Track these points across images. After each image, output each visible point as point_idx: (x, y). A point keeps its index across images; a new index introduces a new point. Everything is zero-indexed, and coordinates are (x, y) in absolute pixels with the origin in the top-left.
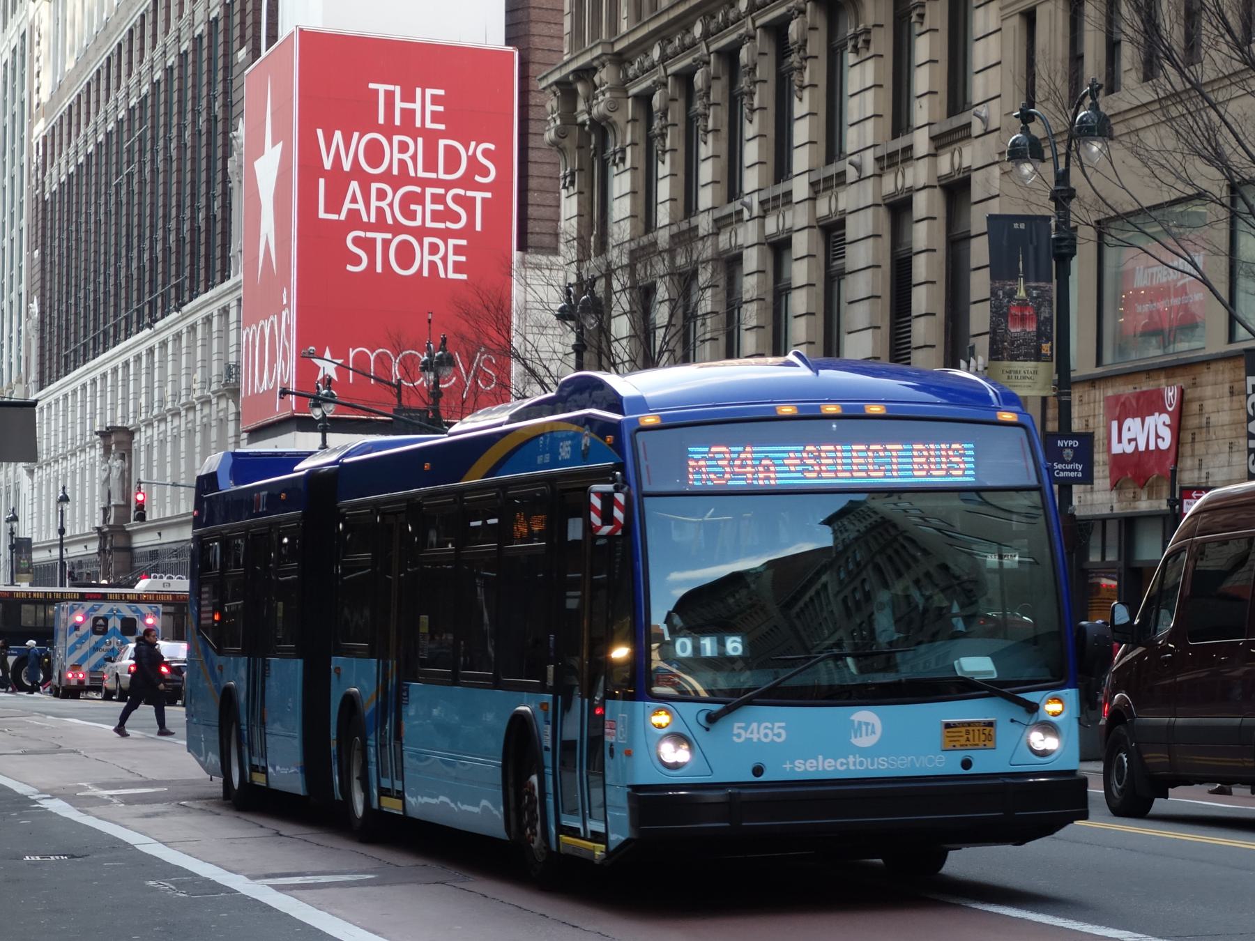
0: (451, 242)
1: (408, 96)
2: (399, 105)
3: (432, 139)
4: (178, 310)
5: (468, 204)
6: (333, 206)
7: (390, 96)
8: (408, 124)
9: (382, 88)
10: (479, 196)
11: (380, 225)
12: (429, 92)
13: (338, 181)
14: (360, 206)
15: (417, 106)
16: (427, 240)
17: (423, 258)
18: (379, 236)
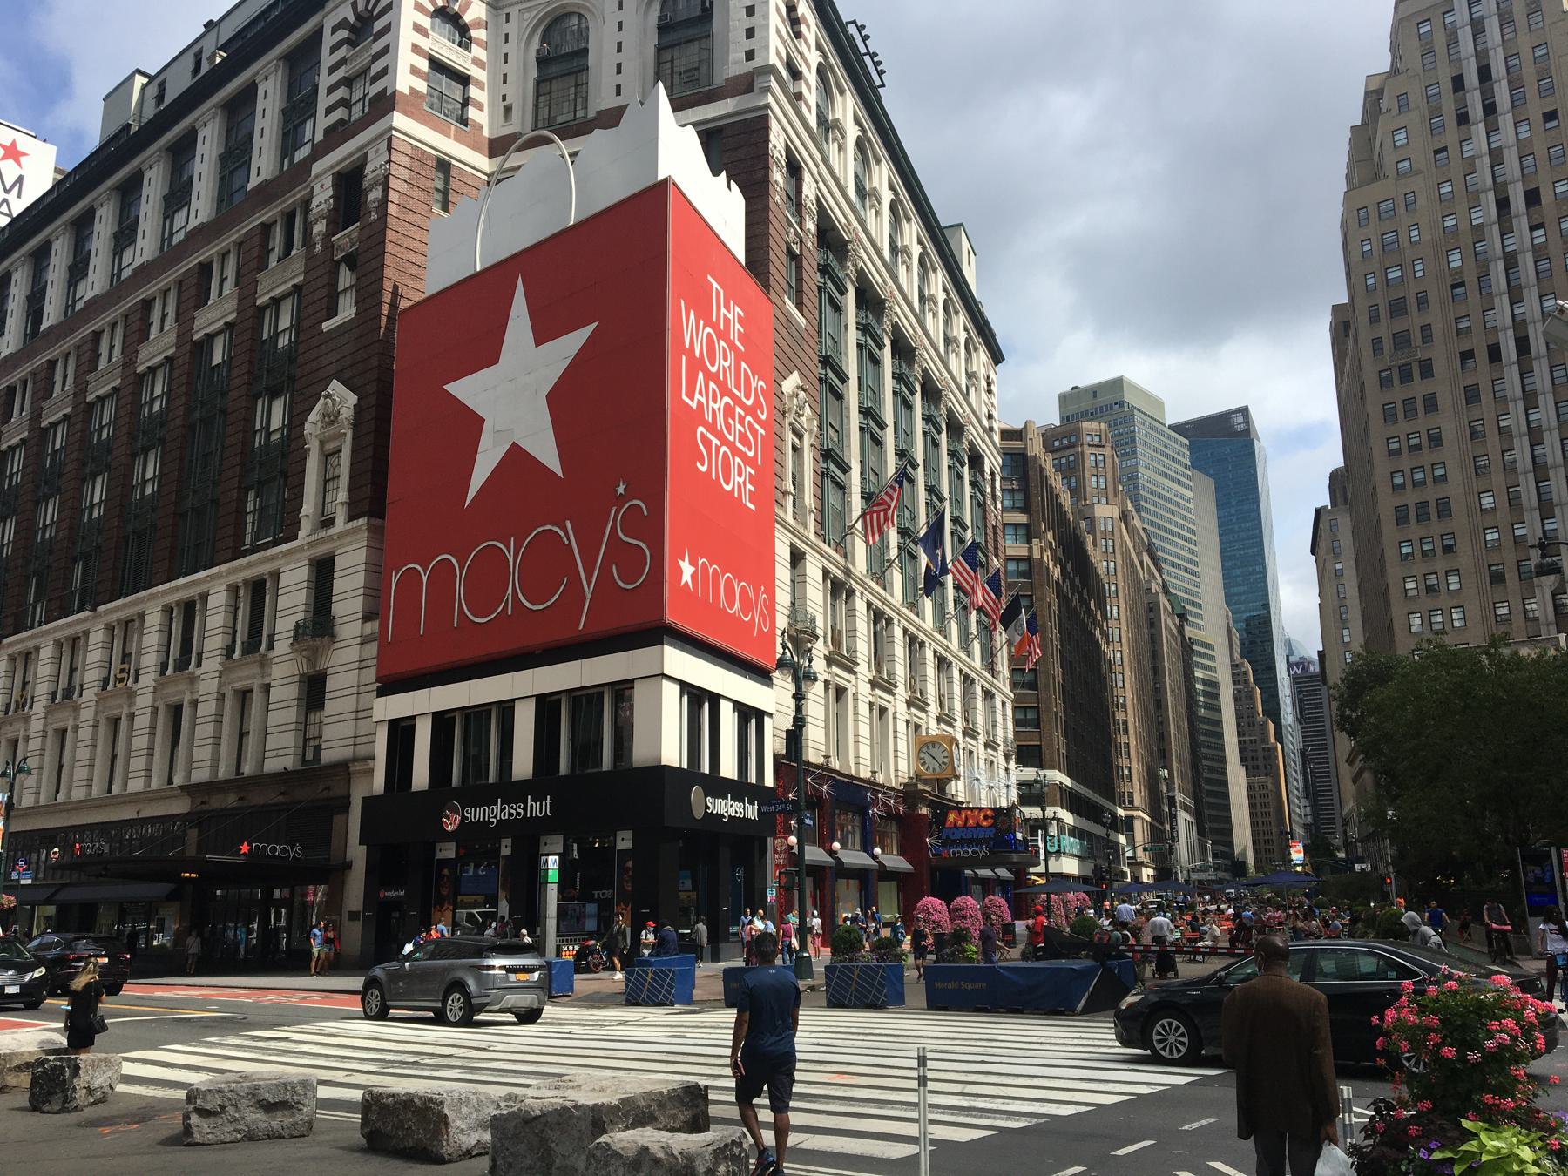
0: (749, 469)
1: (727, 308)
2: (723, 310)
3: (739, 357)
4: (93, 610)
5: (754, 432)
6: (691, 395)
7: (718, 293)
8: (724, 335)
9: (715, 285)
10: (761, 431)
11: (712, 428)
12: (737, 309)
13: (696, 365)
14: (703, 400)
15: (730, 316)
16: (738, 460)
17: (736, 479)
18: (715, 441)
